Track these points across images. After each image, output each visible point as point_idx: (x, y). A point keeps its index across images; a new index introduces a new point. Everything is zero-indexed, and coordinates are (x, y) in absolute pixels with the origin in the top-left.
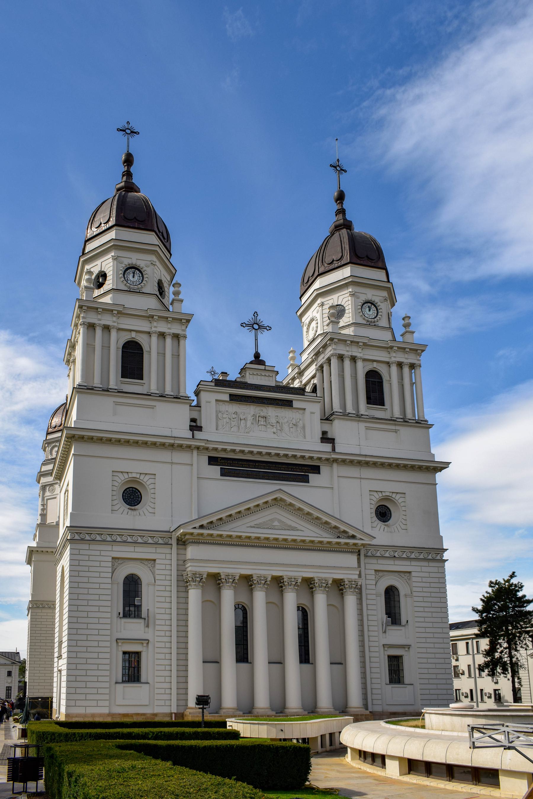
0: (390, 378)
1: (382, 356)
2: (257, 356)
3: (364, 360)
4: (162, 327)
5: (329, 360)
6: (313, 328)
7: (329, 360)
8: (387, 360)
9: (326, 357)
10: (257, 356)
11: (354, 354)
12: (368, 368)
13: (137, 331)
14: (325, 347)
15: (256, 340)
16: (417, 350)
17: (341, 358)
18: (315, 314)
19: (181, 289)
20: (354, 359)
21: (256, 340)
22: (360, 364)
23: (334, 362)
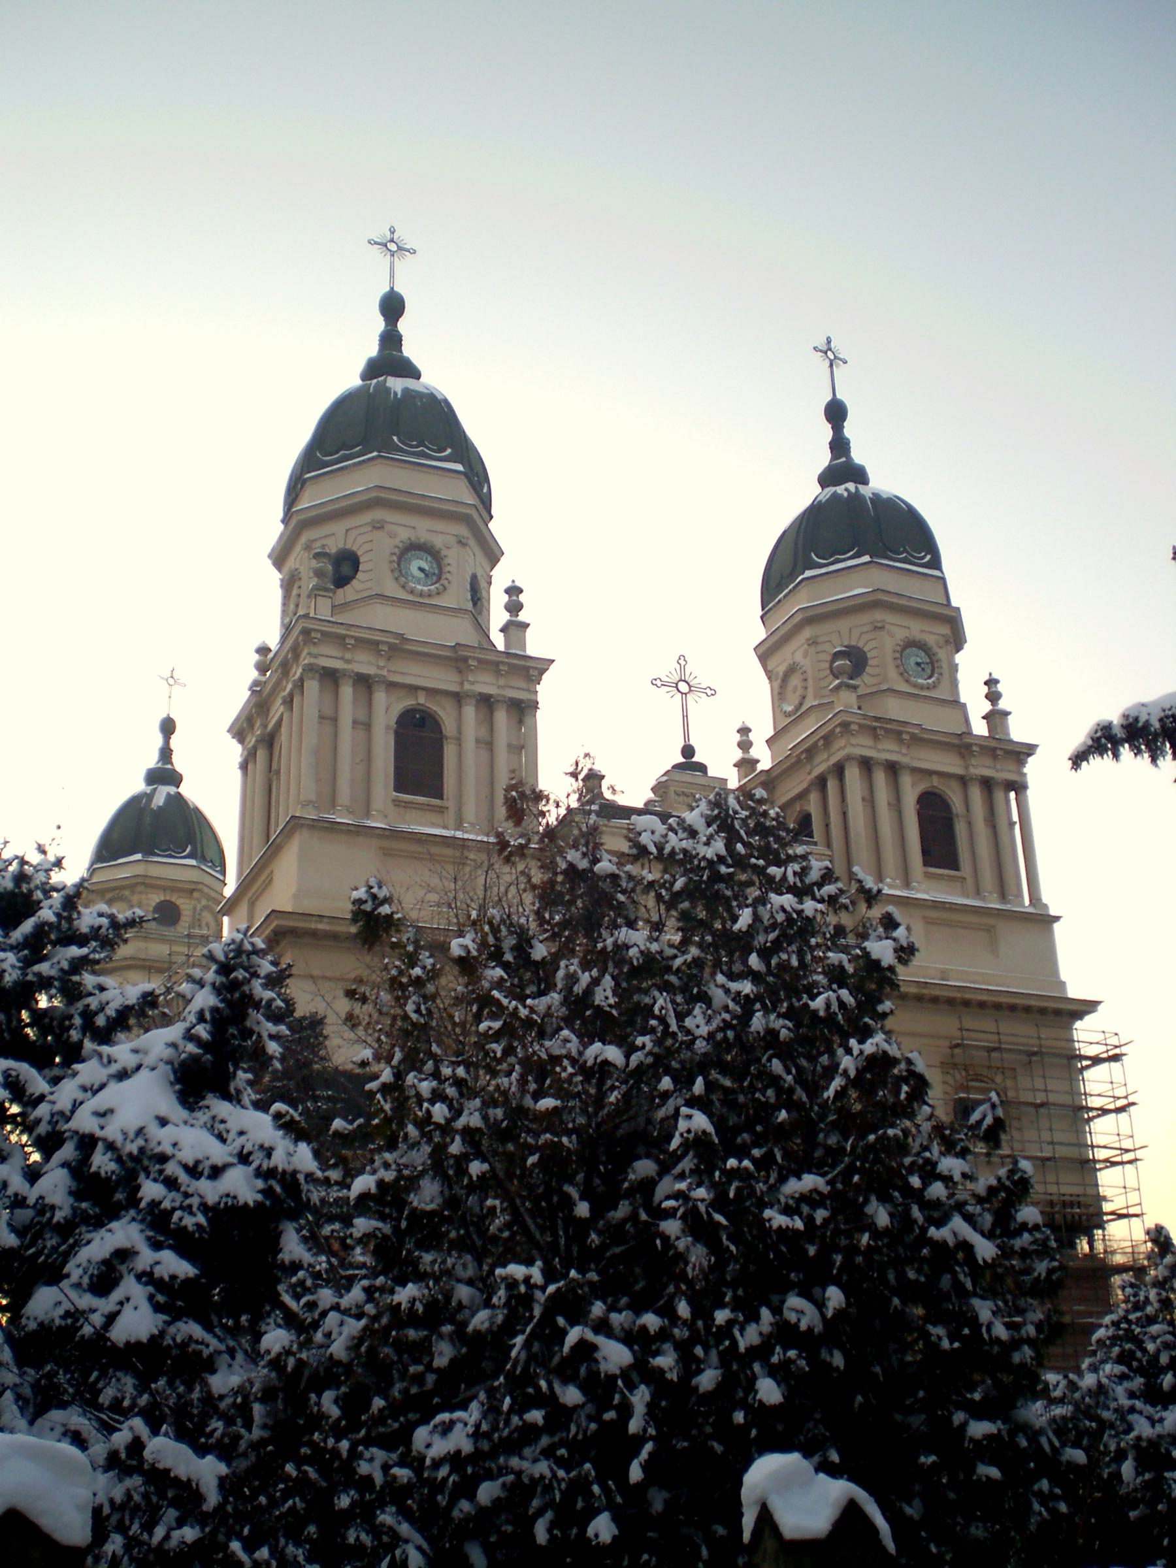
0: (968, 811)
1: (949, 763)
2: (688, 751)
3: (915, 770)
4: (485, 683)
5: (839, 770)
6: (795, 689)
7: (839, 770)
8: (959, 771)
9: (834, 759)
10: (688, 751)
11: (894, 757)
12: (922, 787)
13: (431, 692)
14: (828, 739)
15: (685, 717)
16: (1019, 753)
17: (866, 765)
18: (798, 657)
19: (522, 598)
20: (893, 769)
21: (685, 717)
22: (906, 780)
23: (853, 774)
